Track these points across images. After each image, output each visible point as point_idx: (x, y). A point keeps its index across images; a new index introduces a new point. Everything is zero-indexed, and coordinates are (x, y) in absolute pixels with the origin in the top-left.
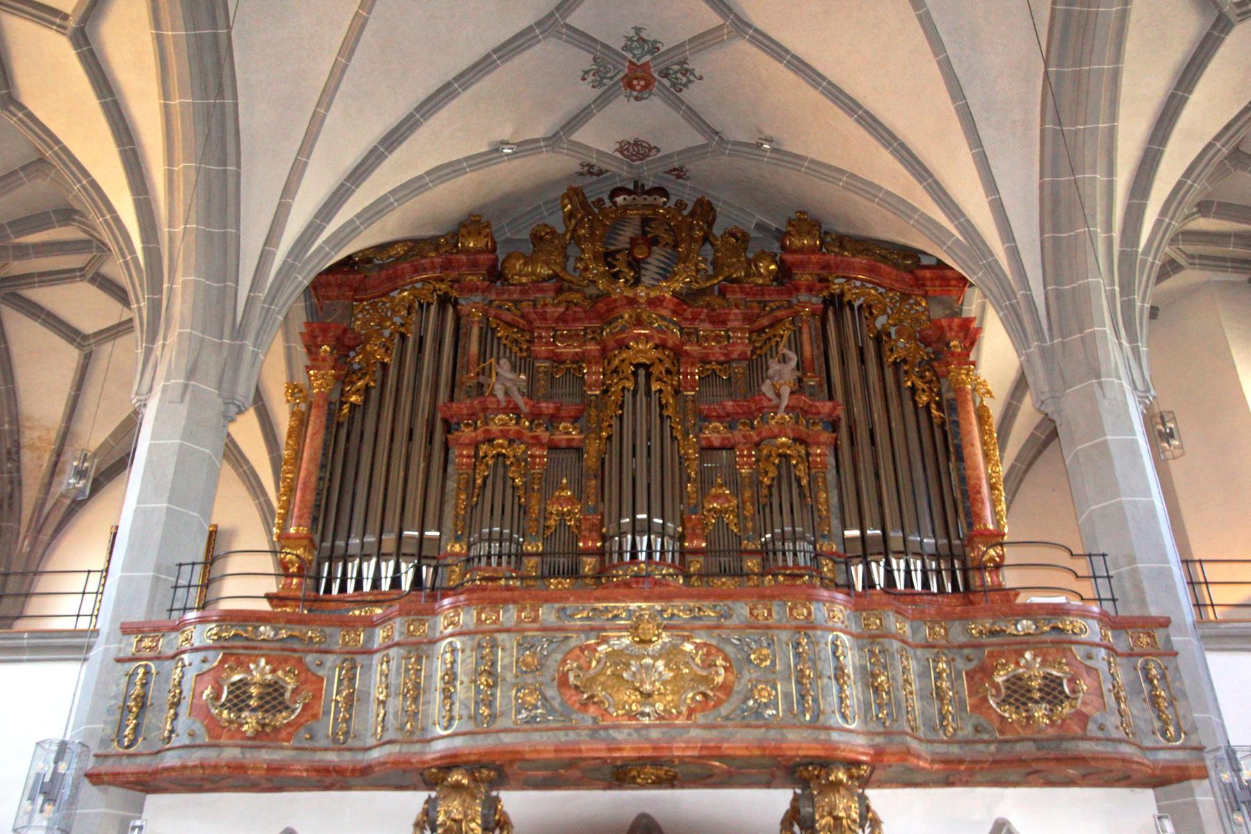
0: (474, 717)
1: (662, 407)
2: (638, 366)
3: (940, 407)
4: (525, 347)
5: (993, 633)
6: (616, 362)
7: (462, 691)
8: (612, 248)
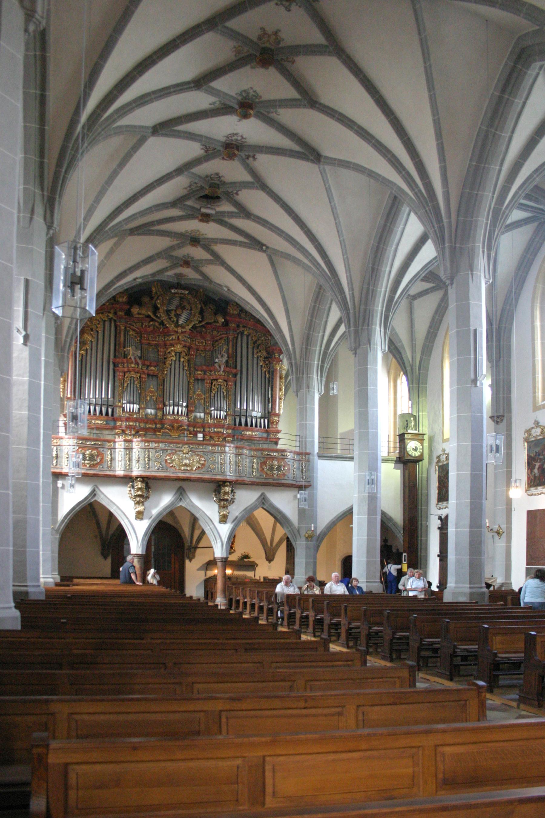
0: (145, 467)
1: (184, 366)
2: (176, 353)
3: (269, 373)
4: (139, 339)
5: (268, 455)
6: (169, 350)
7: (141, 462)
8: (169, 309)
